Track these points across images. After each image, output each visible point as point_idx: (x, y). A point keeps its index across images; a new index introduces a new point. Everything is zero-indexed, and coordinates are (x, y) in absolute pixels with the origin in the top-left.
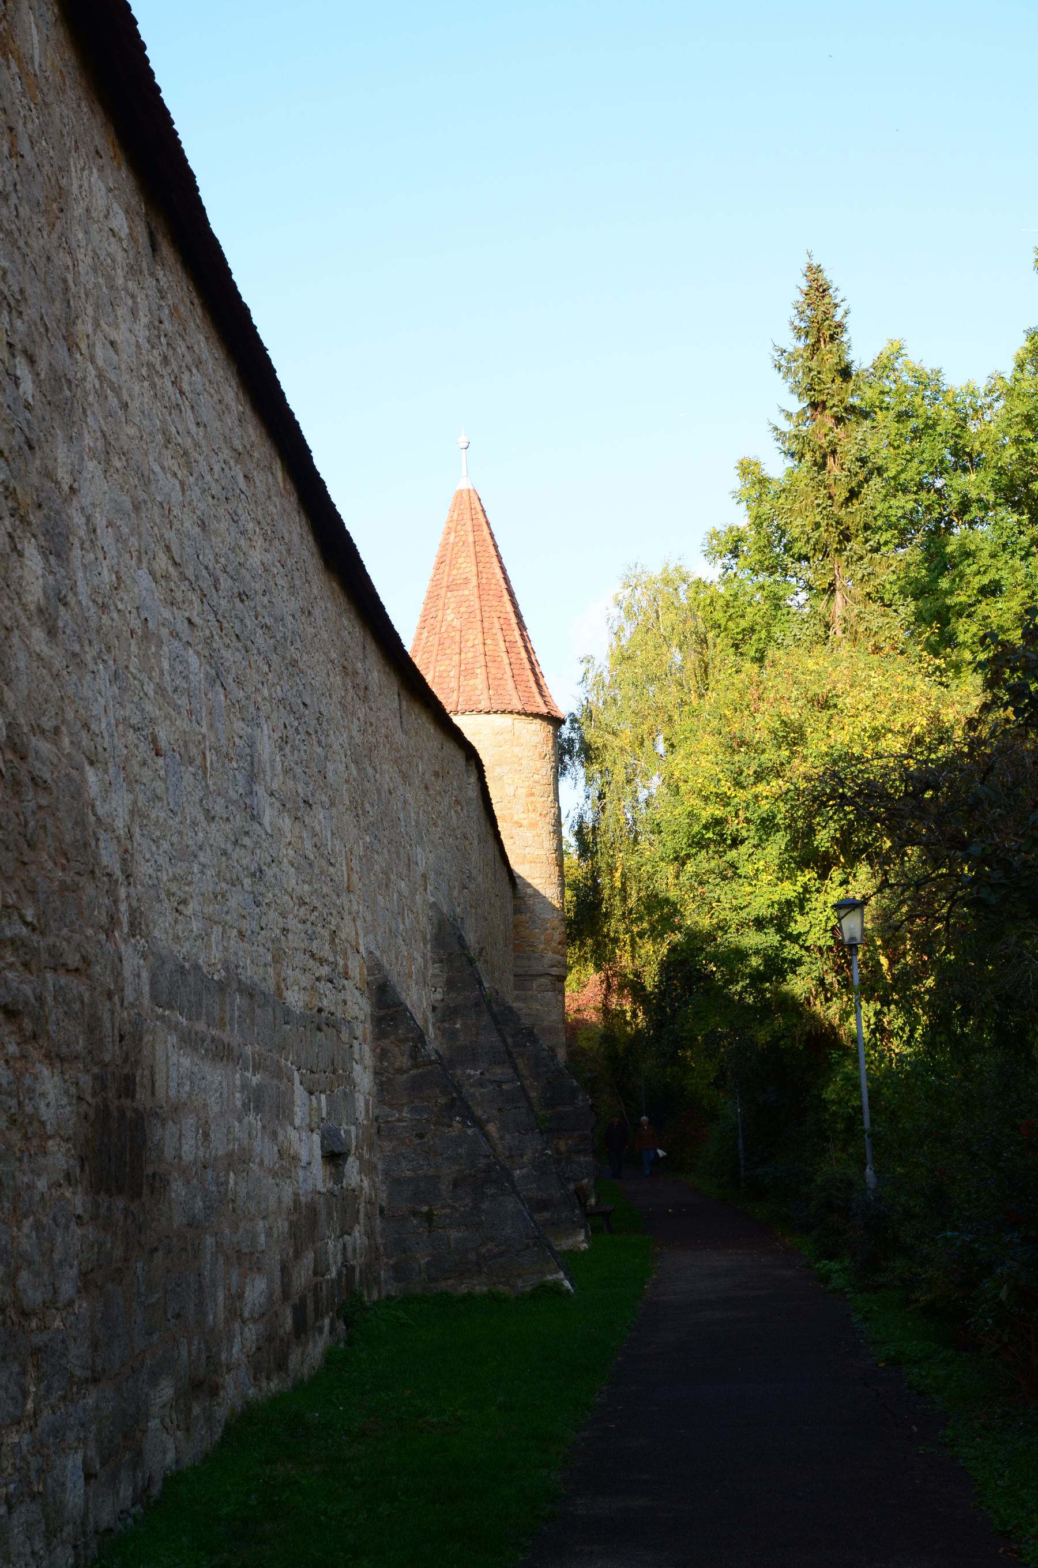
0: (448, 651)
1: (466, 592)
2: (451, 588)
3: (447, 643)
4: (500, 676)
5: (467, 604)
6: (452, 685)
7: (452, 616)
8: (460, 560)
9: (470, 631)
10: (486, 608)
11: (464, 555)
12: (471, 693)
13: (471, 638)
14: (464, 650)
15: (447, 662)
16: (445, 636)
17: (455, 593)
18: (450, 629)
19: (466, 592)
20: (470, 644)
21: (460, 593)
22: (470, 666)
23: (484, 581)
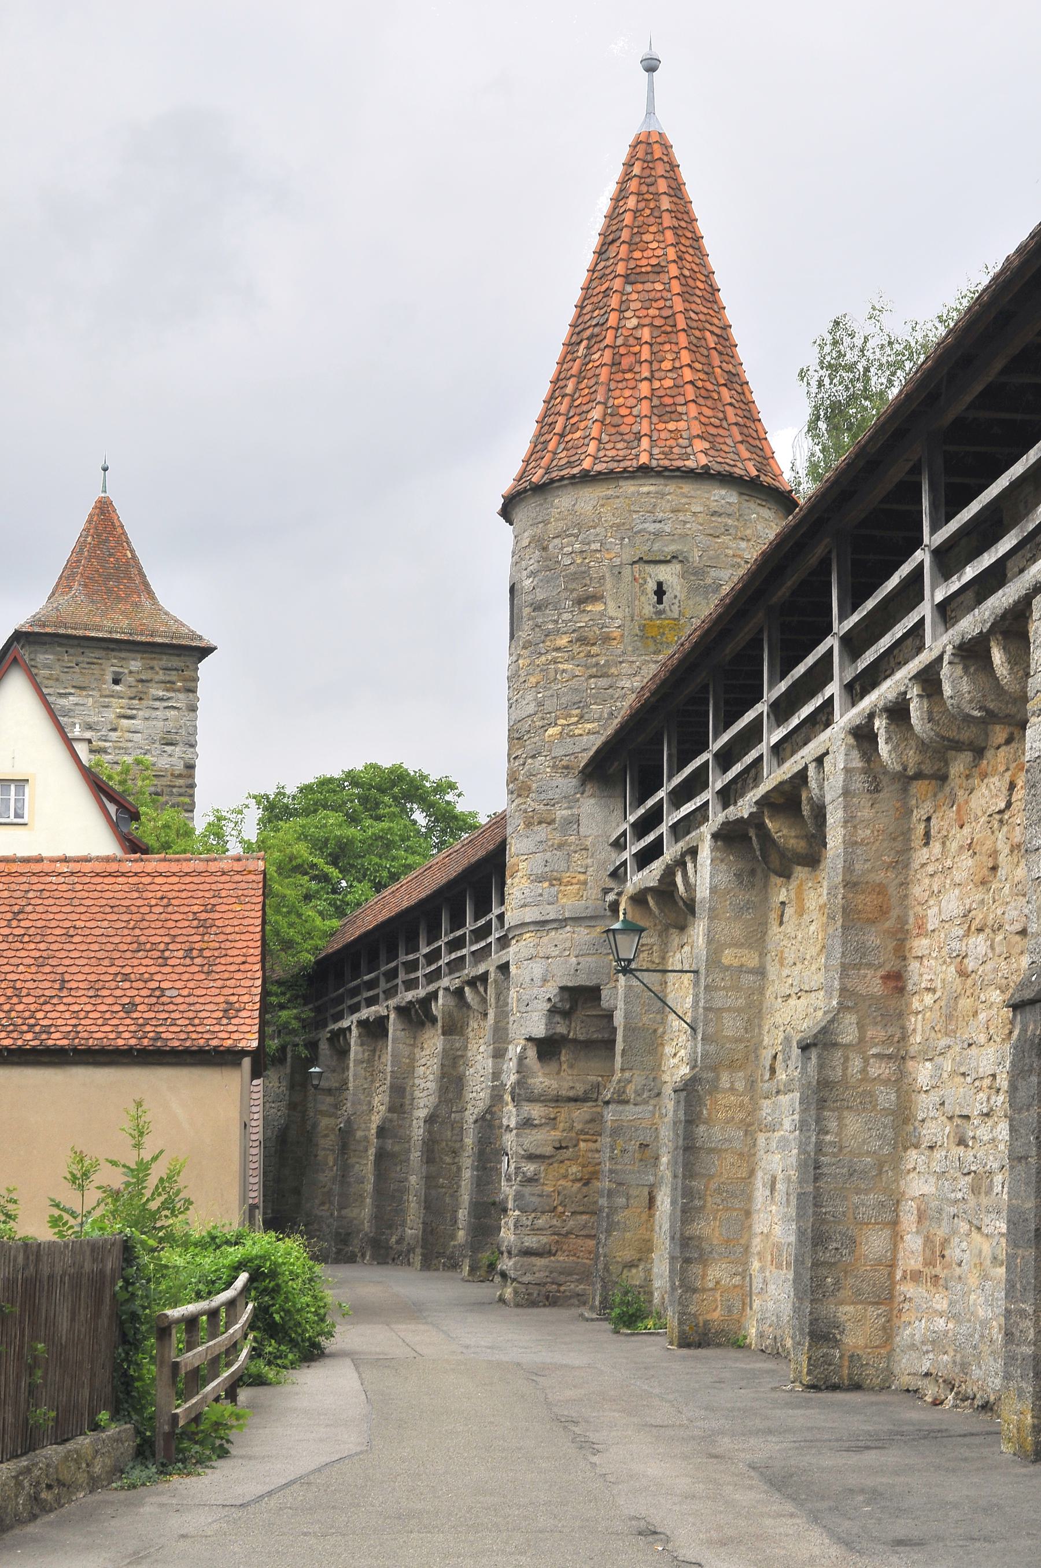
0: (628, 376)
1: (659, 286)
2: (632, 278)
3: (626, 362)
4: (717, 422)
5: (661, 304)
6: (635, 428)
7: (634, 322)
8: (648, 237)
9: (667, 347)
10: (693, 315)
11: (653, 229)
12: (672, 443)
13: (669, 356)
14: (657, 375)
15: (627, 393)
16: (622, 351)
17: (640, 287)
18: (632, 341)
19: (659, 286)
20: (667, 365)
21: (648, 286)
22: (668, 401)
23: (687, 273)
